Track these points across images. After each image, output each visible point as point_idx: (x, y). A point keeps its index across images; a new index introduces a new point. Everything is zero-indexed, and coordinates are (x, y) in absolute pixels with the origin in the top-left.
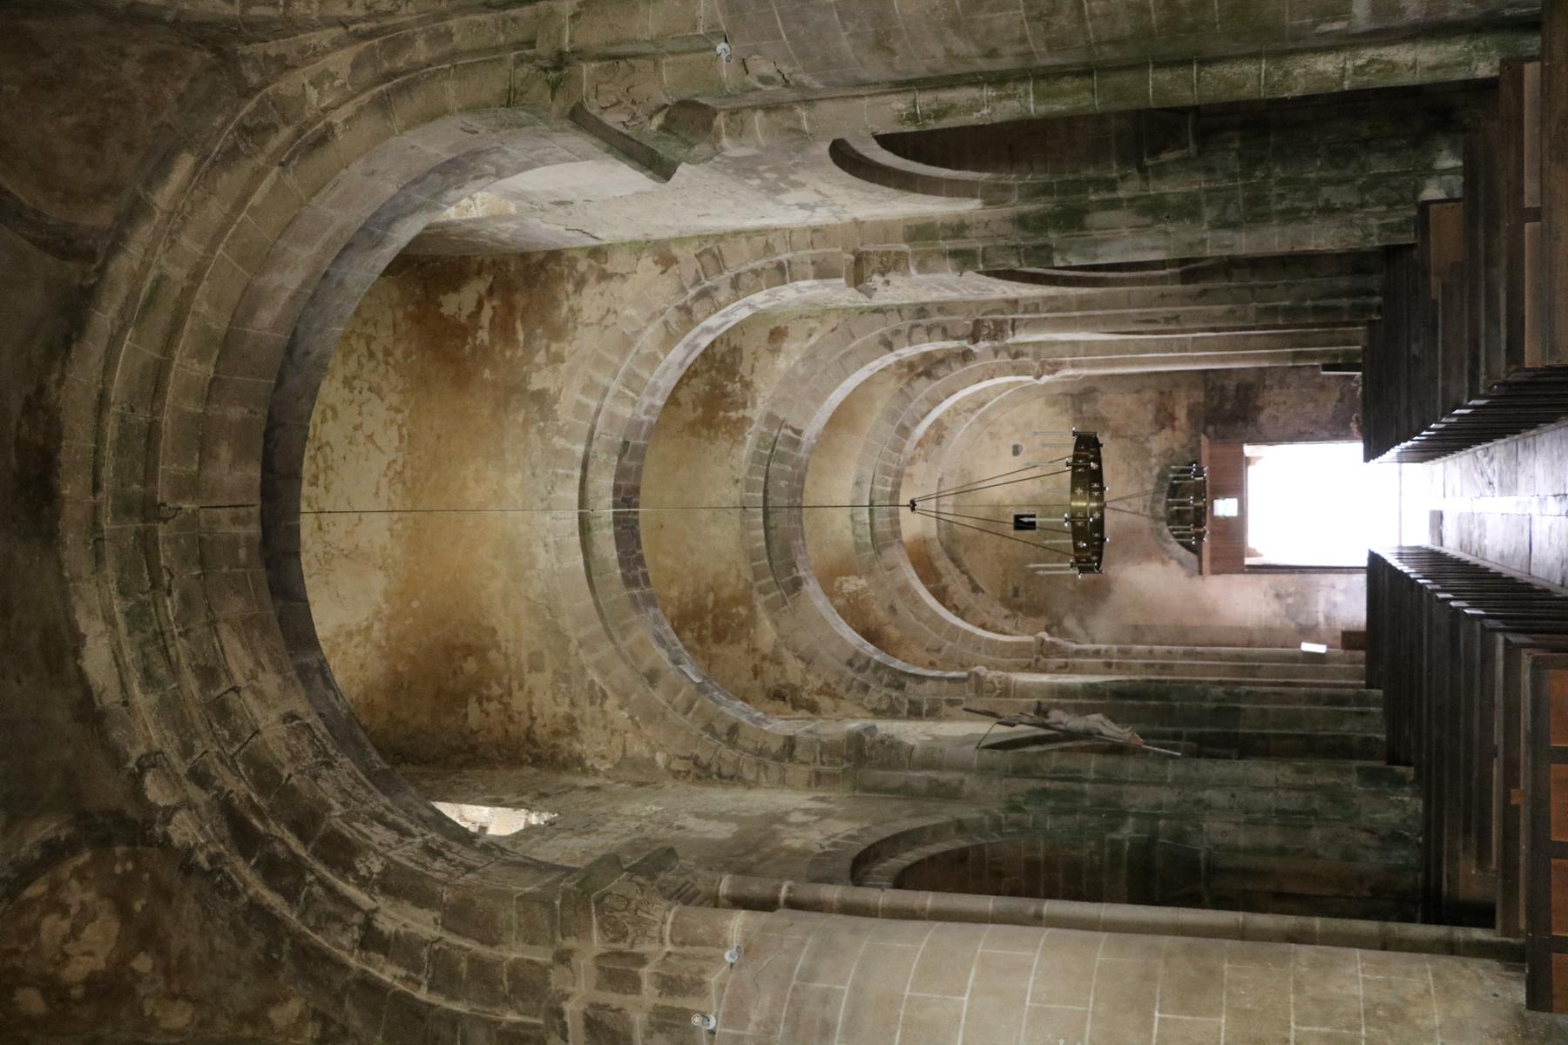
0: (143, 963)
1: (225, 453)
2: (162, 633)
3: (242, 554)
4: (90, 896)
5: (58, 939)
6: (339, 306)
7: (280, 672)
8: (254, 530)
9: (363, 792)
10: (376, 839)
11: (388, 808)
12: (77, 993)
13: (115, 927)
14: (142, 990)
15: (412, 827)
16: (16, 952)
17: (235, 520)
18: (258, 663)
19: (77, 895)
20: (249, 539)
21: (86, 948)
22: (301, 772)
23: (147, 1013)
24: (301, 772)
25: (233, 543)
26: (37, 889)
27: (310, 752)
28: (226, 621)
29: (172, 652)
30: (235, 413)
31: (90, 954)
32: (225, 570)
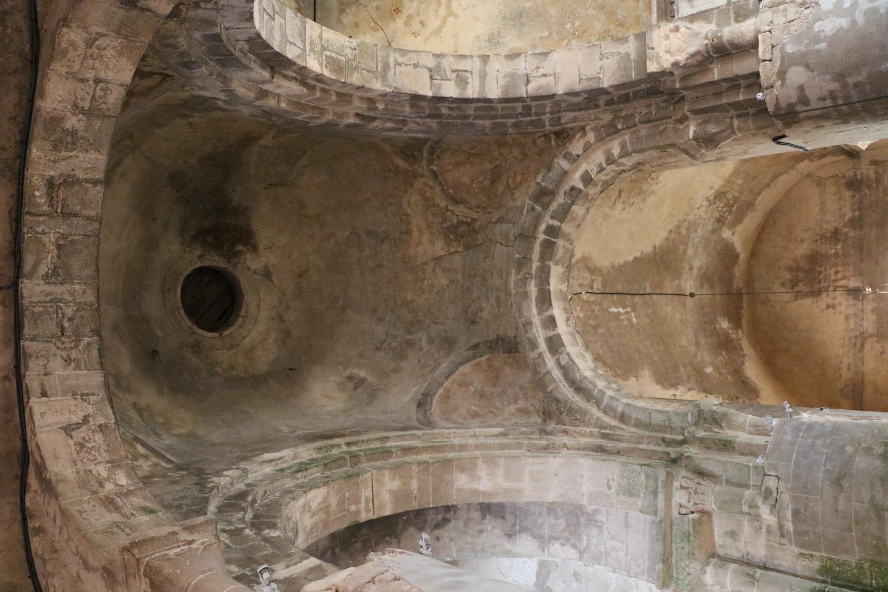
1: (396, 484)
3: (353, 508)
6: (467, 543)
8: (364, 517)
17: (367, 500)
20: (358, 512)
25: (357, 502)
26: (140, 449)
28: (328, 493)
29: (299, 475)
30: (414, 485)
32: (347, 495)
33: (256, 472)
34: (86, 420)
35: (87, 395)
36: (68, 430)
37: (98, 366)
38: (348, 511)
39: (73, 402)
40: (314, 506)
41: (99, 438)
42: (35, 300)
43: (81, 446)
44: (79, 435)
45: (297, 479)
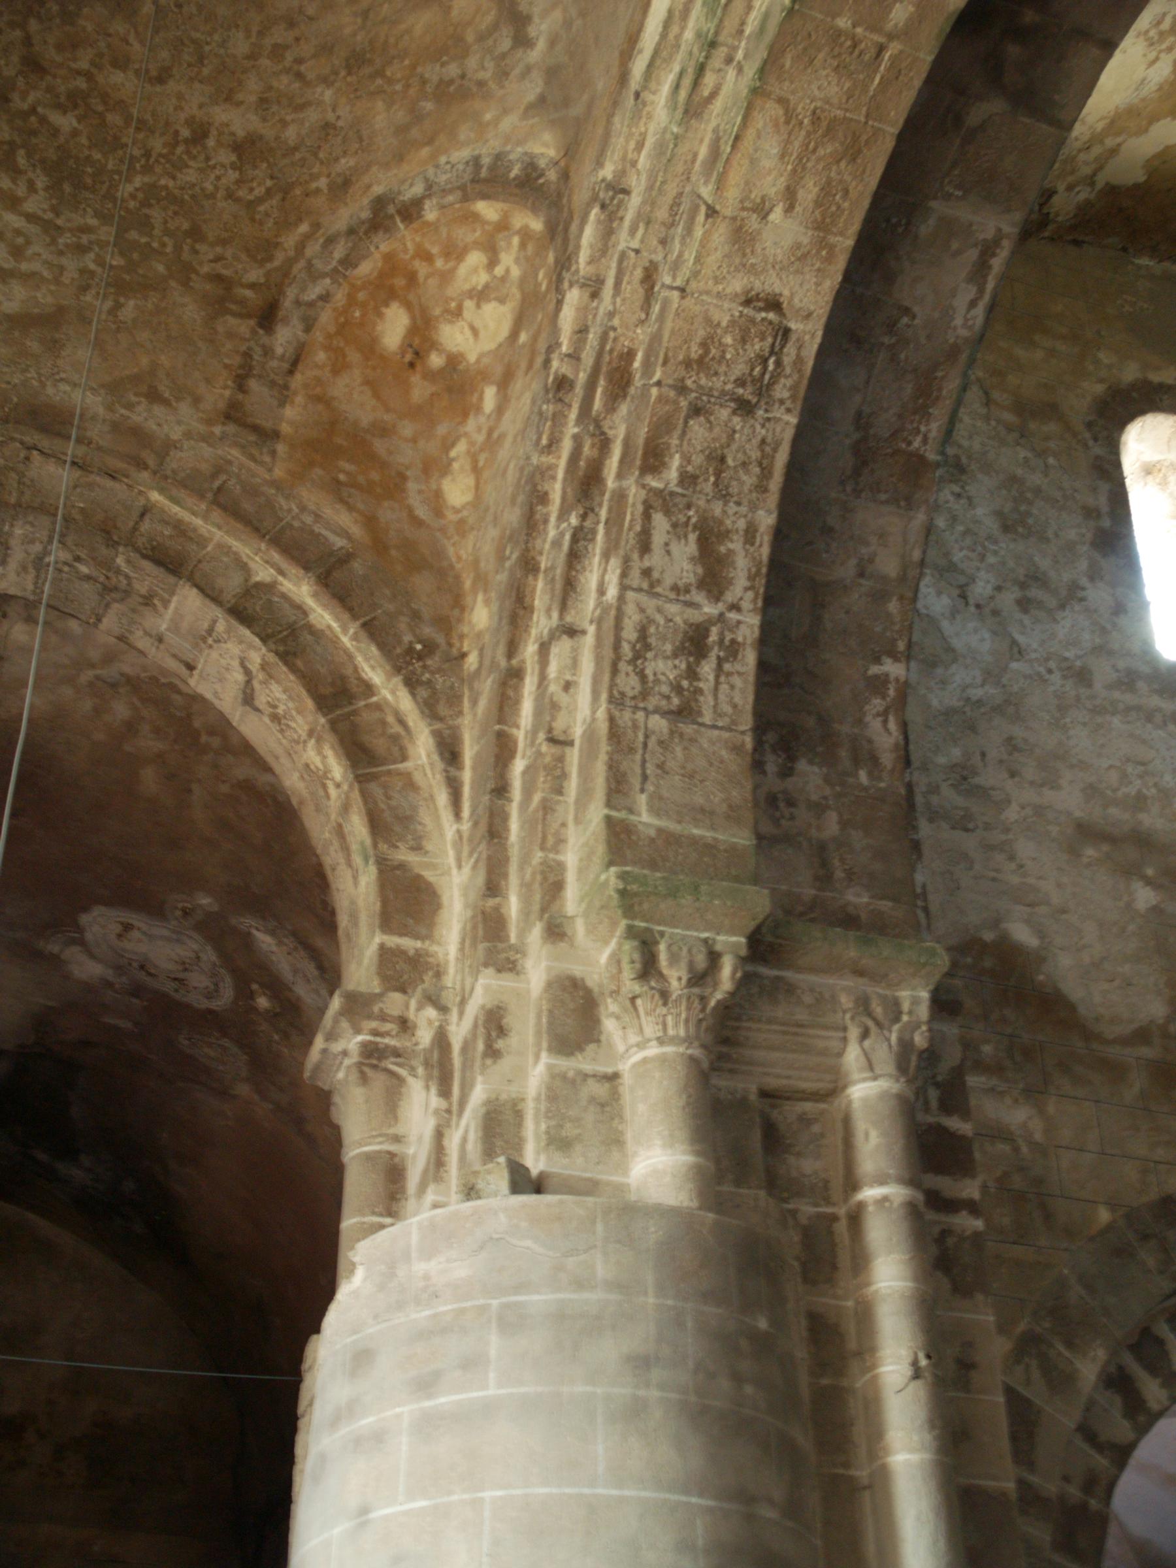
0: (490, 397)
2: (713, 45)
4: (516, 272)
5: (467, 287)
7: (822, 226)
9: (749, 480)
10: (655, 559)
11: (750, 534)
12: (436, 361)
13: (505, 331)
14: (471, 425)
15: (741, 582)
16: (429, 258)
18: (790, 196)
19: (509, 262)
21: (478, 324)
22: (682, 389)
23: (453, 454)
24: (682, 389)
26: (489, 210)
27: (739, 369)
28: (781, 101)
29: (709, 80)
31: (475, 331)
32: (843, 23)
33: (640, 146)
34: (247, 672)
35: (210, 631)
36: (248, 699)
37: (172, 579)
38: (891, 37)
39: (214, 655)
40: (771, 185)
41: (277, 691)
42: (30, 587)
43: (275, 718)
44: (261, 700)
45: (714, 95)
